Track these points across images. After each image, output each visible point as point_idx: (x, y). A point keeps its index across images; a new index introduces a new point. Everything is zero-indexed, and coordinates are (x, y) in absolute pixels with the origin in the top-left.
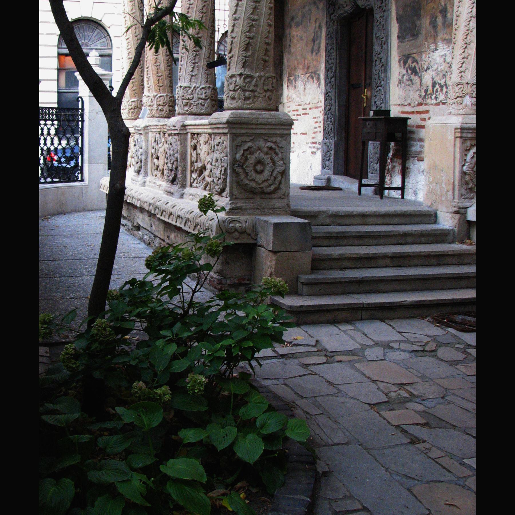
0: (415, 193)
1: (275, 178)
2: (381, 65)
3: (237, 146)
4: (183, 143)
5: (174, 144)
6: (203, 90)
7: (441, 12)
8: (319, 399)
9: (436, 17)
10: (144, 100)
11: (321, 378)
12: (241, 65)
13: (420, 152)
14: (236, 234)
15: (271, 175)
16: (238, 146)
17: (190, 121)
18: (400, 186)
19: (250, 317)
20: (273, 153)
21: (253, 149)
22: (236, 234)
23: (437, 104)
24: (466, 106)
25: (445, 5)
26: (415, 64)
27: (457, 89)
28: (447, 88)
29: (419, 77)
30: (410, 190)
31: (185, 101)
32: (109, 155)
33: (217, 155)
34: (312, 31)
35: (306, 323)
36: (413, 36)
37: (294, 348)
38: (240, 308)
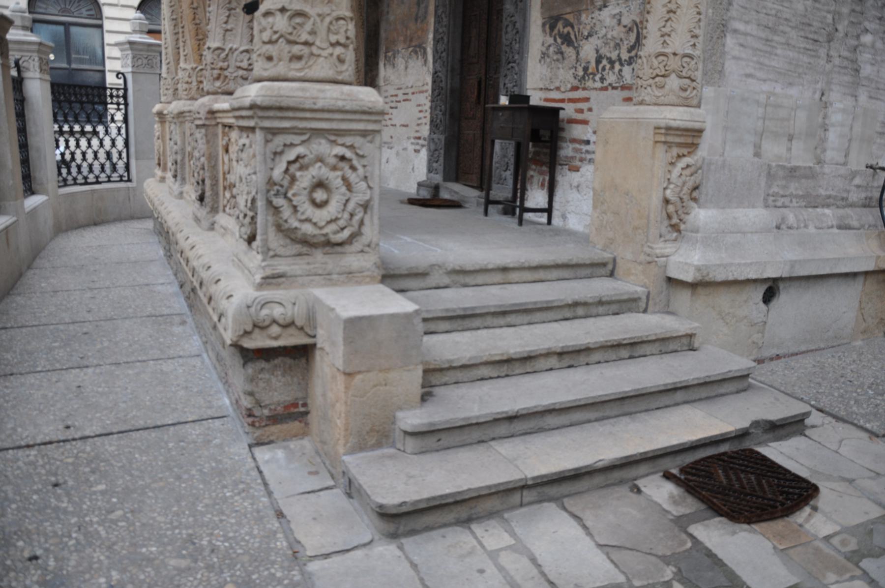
0: (564, 217)
1: (352, 215)
2: (514, 32)
3: (275, 153)
4: (210, 140)
5: (200, 142)
6: (245, 54)
15: (344, 210)
21: (306, 160)
23: (606, 89)
26: (569, 29)
27: (655, 63)
29: (575, 48)
31: (216, 72)
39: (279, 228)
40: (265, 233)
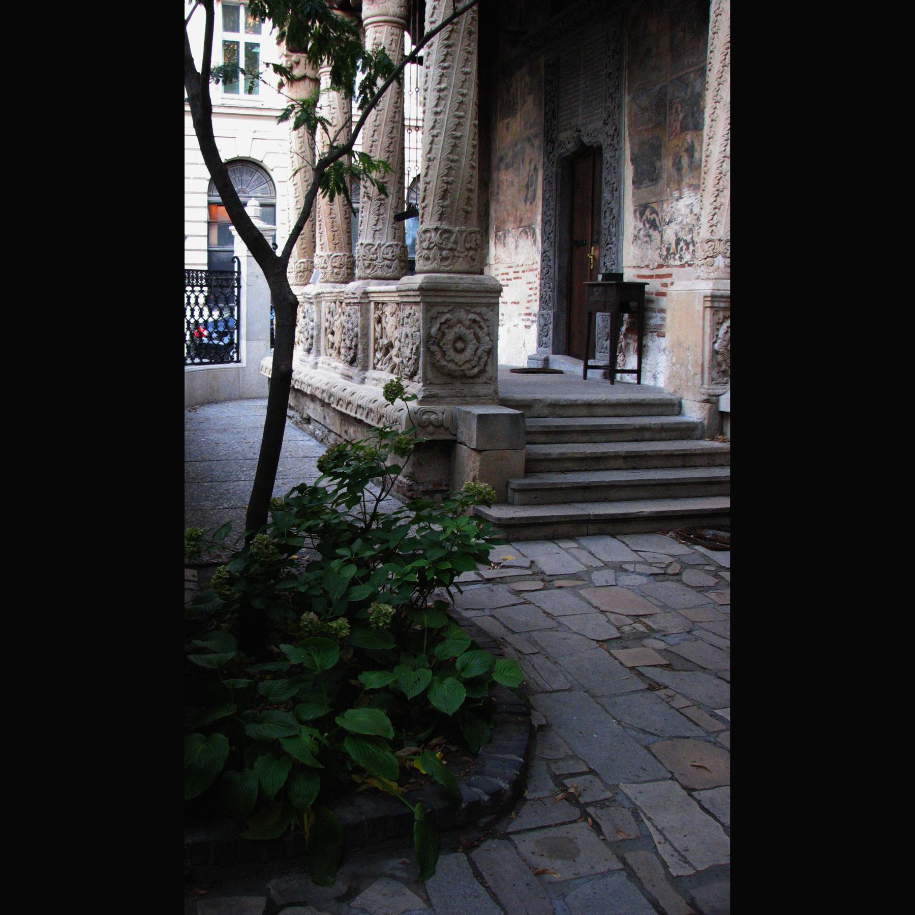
0: (655, 377)
5: (353, 316)
7: (686, 150)
8: (534, 634)
9: (681, 157)
11: (537, 609)
12: (437, 216)
13: (661, 325)
14: (431, 429)
16: (434, 319)
17: (373, 287)
18: (636, 368)
19: (449, 532)
22: (431, 429)
23: (682, 266)
26: (654, 215)
28: (694, 246)
29: (660, 232)
30: (648, 374)
31: (367, 262)
32: (272, 329)
34: (525, 175)
35: (518, 540)
36: (652, 180)
37: (503, 570)
38: (435, 520)
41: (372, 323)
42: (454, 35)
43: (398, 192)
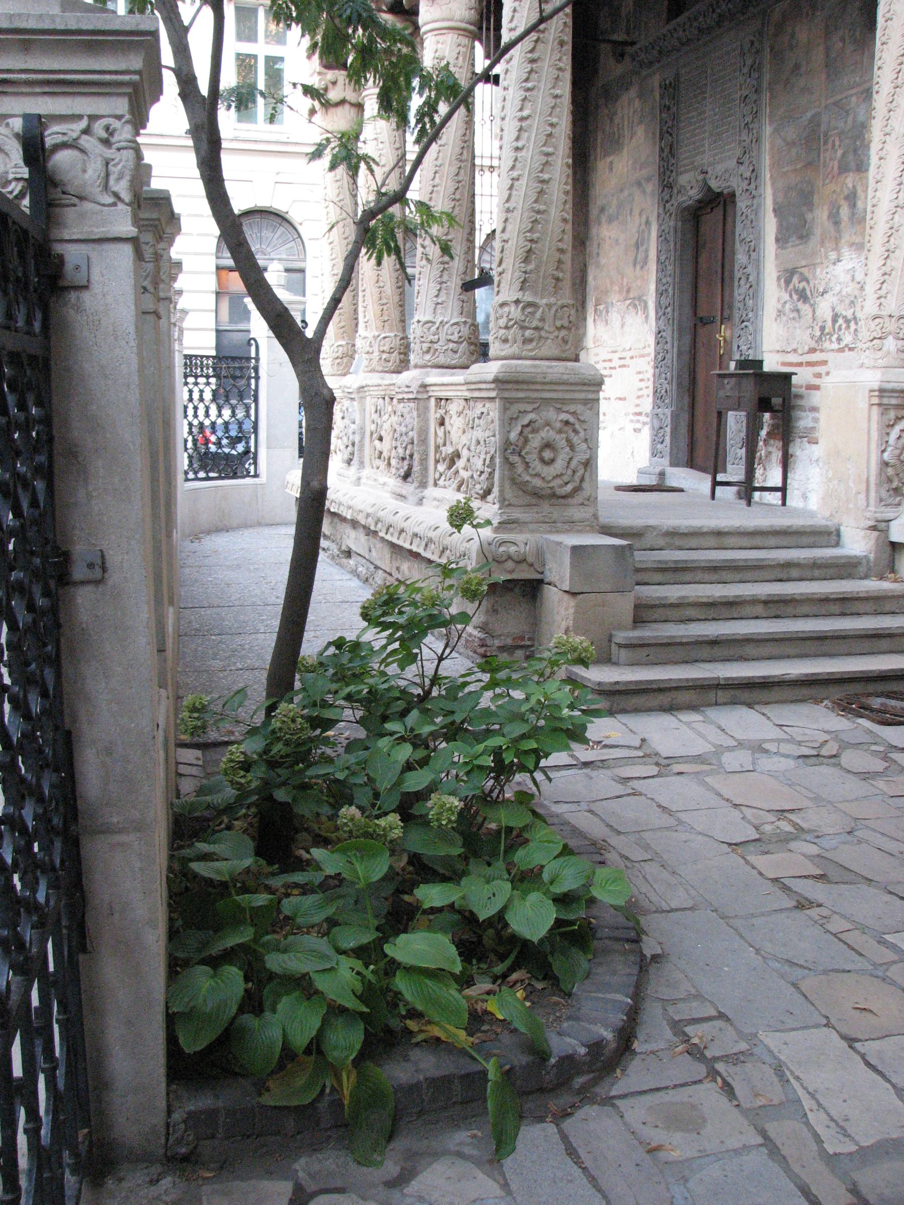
0: (805, 497)
1: (574, 472)
3: (511, 419)
4: (423, 414)
7: (847, 198)
8: (645, 835)
10: (359, 343)
11: (649, 802)
13: (813, 428)
14: (510, 565)
17: (434, 377)
18: (780, 485)
19: (533, 700)
20: (570, 431)
21: (537, 424)
23: (841, 350)
24: (889, 353)
25: (854, 187)
26: (804, 284)
27: (873, 325)
28: (856, 324)
29: (812, 305)
30: (796, 492)
33: (478, 434)
34: (634, 230)
35: (624, 711)
36: (801, 237)
37: (606, 751)
38: (516, 685)
39: (513, 481)
40: (502, 486)
41: (432, 425)
42: (540, 46)
43: (466, 253)
